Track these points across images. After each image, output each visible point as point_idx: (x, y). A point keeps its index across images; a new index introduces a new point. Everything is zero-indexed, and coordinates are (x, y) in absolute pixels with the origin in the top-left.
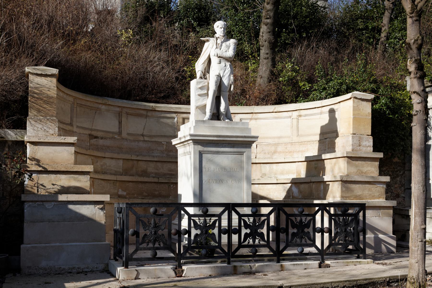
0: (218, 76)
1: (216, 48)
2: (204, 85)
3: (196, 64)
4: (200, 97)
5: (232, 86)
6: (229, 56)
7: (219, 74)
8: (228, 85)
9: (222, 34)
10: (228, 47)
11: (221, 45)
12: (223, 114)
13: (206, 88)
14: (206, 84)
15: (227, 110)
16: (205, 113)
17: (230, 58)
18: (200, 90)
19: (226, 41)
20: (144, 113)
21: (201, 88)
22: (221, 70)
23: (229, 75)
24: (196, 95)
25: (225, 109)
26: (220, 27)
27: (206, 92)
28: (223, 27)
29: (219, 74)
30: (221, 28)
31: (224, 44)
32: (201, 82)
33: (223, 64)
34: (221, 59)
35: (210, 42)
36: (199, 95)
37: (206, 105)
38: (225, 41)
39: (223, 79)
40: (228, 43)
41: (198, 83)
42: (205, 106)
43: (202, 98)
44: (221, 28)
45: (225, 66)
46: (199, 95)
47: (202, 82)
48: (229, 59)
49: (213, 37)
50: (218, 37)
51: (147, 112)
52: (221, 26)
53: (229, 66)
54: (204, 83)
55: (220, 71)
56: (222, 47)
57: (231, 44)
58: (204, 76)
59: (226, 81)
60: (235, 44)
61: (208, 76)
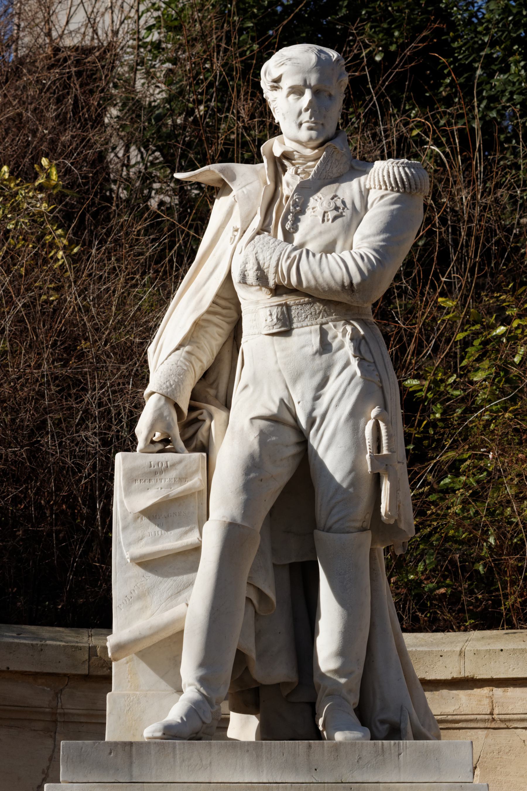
0: (272, 419)
1: (263, 229)
2: (178, 489)
3: (150, 350)
4: (151, 578)
5: (386, 486)
6: (340, 274)
7: (286, 406)
8: (352, 484)
10: (349, 217)
11: (300, 209)
12: (335, 693)
15: (368, 652)
16: (180, 691)
17: (350, 288)
18: (153, 528)
19: (338, 179)
20: (38, 697)
22: (297, 377)
23: (356, 414)
25: (344, 651)
26: (286, 84)
28: (313, 79)
29: (286, 406)
30: (297, 91)
31: (319, 203)
32: (155, 473)
33: (306, 336)
34: (291, 300)
35: (235, 187)
37: (182, 632)
38: (326, 178)
39: (313, 441)
40: (349, 190)
42: (178, 637)
43: (168, 584)
44: (297, 91)
45: (325, 347)
48: (344, 298)
49: (255, 159)
50: (287, 156)
51: (57, 694)
52: (297, 80)
53: (349, 348)
54: (182, 479)
55: (306, 383)
56: (306, 221)
57: (373, 195)
58: (191, 430)
59: (333, 454)
60: (405, 189)
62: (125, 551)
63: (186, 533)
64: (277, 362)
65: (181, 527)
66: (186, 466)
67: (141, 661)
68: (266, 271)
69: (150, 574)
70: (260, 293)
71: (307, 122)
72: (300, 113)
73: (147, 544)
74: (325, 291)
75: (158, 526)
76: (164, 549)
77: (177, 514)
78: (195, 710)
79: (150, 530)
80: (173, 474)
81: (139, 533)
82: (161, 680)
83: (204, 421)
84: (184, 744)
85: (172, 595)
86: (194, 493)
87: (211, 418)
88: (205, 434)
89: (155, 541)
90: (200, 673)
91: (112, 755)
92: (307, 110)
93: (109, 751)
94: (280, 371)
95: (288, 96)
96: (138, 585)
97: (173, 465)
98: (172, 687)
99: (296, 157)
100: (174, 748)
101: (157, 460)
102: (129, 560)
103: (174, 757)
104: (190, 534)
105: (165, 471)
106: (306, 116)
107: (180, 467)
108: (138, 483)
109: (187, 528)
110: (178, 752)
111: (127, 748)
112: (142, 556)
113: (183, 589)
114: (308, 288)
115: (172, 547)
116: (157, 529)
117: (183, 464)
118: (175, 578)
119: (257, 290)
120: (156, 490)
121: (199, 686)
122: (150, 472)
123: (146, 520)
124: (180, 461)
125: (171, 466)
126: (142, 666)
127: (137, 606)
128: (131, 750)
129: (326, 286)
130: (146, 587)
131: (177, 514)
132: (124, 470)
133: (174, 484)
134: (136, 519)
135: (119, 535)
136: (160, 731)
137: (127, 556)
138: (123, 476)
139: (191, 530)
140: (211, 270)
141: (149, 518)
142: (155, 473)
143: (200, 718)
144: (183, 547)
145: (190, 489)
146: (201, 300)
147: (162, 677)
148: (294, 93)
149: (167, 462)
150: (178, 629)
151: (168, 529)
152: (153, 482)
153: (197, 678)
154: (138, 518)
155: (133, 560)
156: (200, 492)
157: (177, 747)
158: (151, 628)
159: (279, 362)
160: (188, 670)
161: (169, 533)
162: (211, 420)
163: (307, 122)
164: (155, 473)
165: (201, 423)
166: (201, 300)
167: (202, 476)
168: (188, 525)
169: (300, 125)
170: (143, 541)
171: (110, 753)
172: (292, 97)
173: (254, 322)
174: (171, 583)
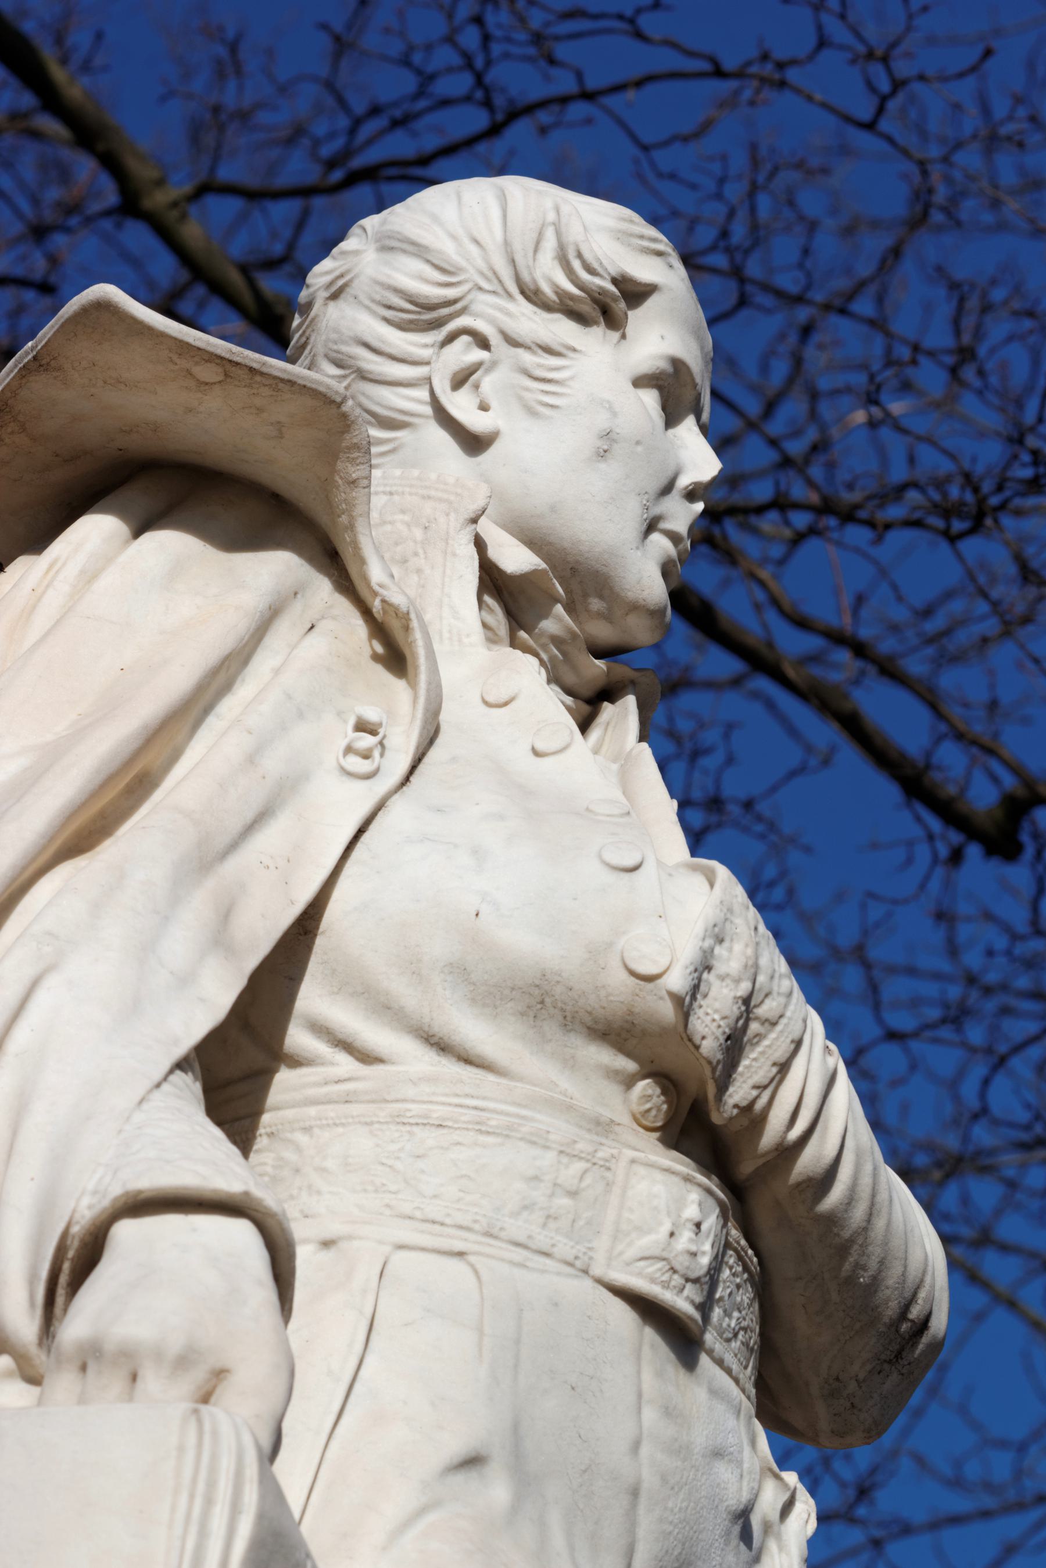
9: (644, 575)
64: (636, 1446)
68: (754, 1027)
70: (612, 1091)
71: (674, 537)
72: (667, 489)
74: (850, 1281)
92: (691, 495)
94: (635, 1493)
95: (640, 382)
99: (548, 626)
106: (682, 515)
114: (832, 1221)
119: (613, 1074)
129: (873, 1264)
140: (249, 815)
146: (226, 914)
148: (660, 388)
159: (645, 1450)
163: (674, 537)
166: (226, 914)
169: (652, 526)
172: (650, 398)
173: (565, 1201)
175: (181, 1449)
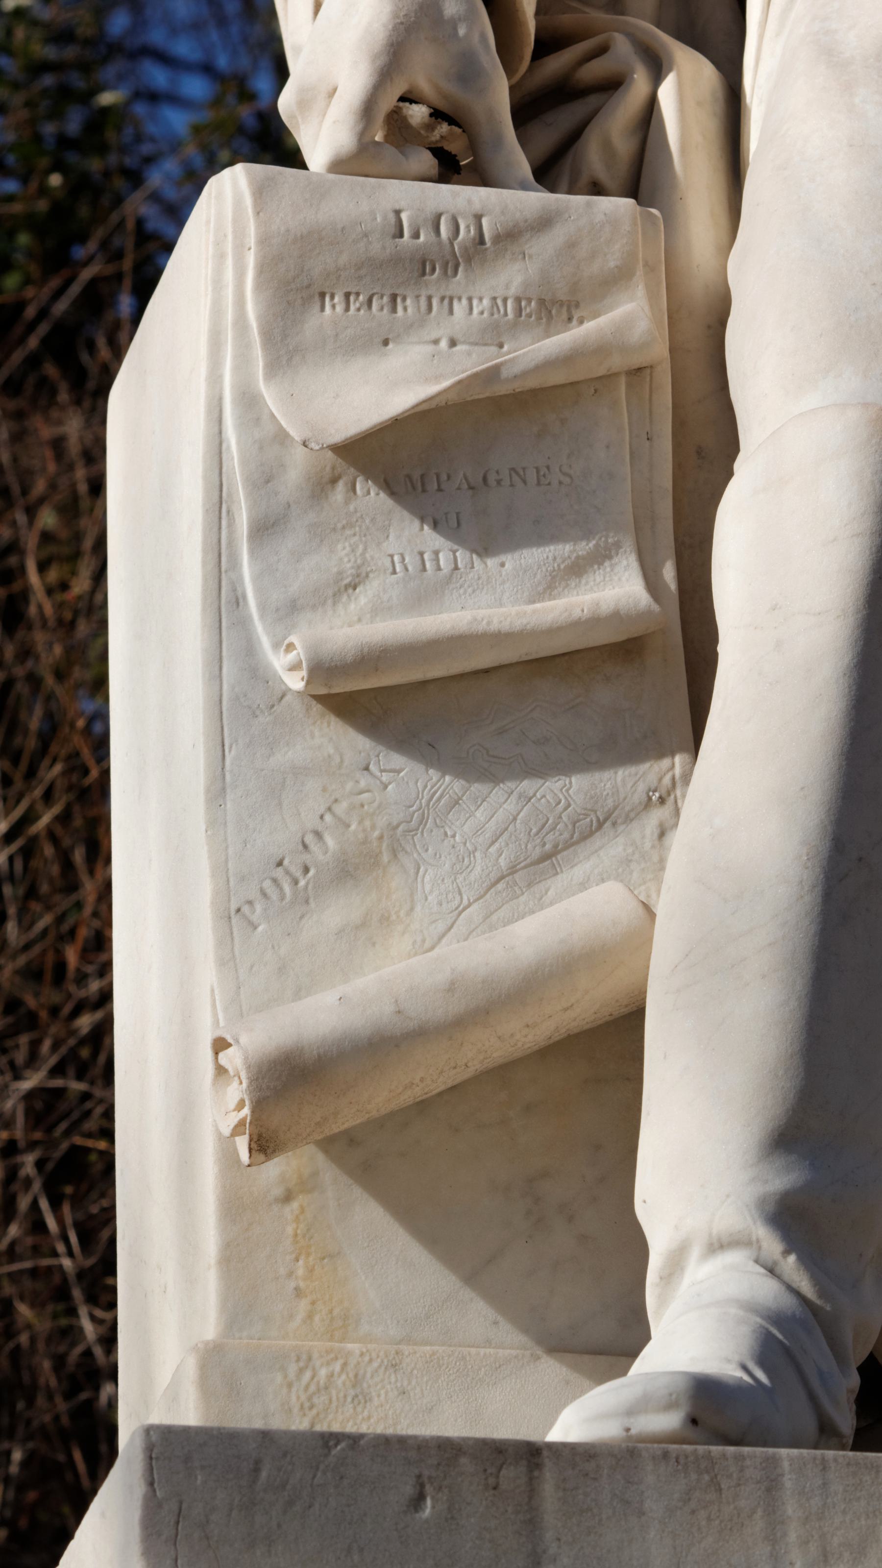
2: (533, 350)
4: (403, 780)
13: (633, 450)
14: (629, 317)
18: (407, 539)
21: (437, 466)
24: (239, 706)
27: (619, 589)
32: (420, 268)
36: (392, 703)
41: (300, 288)
43: (491, 814)
46: (392, 703)
47: (478, 251)
54: (554, 306)
61: (680, 96)
62: (265, 641)
63: (577, 570)
65: (553, 539)
66: (572, 245)
67: (357, 1192)
69: (397, 760)
73: (378, 610)
75: (435, 525)
76: (482, 627)
77: (531, 476)
78: (787, 1351)
79: (393, 545)
80: (510, 277)
81: (340, 556)
82: (467, 1294)
83: (614, 84)
84: (824, 1466)
85: (513, 870)
86: (610, 377)
87: (658, 68)
88: (624, 146)
89: (421, 598)
90: (780, 1180)
91: (428, 1510)
93: (409, 1490)
96: (340, 809)
97: (511, 236)
98: (526, 1331)
100: (771, 1484)
101: (432, 207)
102: (296, 682)
103: (773, 1536)
104: (596, 576)
105: (469, 260)
107: (543, 248)
108: (333, 310)
109: (584, 547)
110: (791, 1508)
111: (512, 1475)
112: (373, 658)
113: (569, 844)
115: (519, 624)
116: (431, 539)
117: (557, 236)
118: (527, 785)
120: (430, 348)
121: (771, 1244)
122: (396, 261)
123: (371, 497)
124: (544, 223)
125: (498, 238)
126: (368, 1216)
127: (335, 913)
128: (532, 1489)
130: (382, 821)
131: (531, 476)
132: (263, 241)
133: (514, 326)
134: (321, 486)
135: (235, 564)
136: (670, 1406)
137: (278, 662)
138: (261, 270)
139: (601, 557)
141: (389, 487)
142: (423, 266)
143: (812, 1397)
144: (576, 624)
145: (600, 349)
147: (471, 1278)
149: (478, 218)
150: (587, 1002)
151: (487, 545)
152: (409, 309)
153: (761, 1203)
154: (334, 481)
155: (321, 670)
156: (636, 373)
157: (788, 1482)
158: (451, 987)
160: (697, 1176)
161: (492, 562)
162: (657, 77)
164: (423, 266)
165: (592, 100)
167: (652, 296)
168: (587, 535)
170: (363, 597)
171: (418, 1500)
174: (510, 806)
175: (208, 222)
